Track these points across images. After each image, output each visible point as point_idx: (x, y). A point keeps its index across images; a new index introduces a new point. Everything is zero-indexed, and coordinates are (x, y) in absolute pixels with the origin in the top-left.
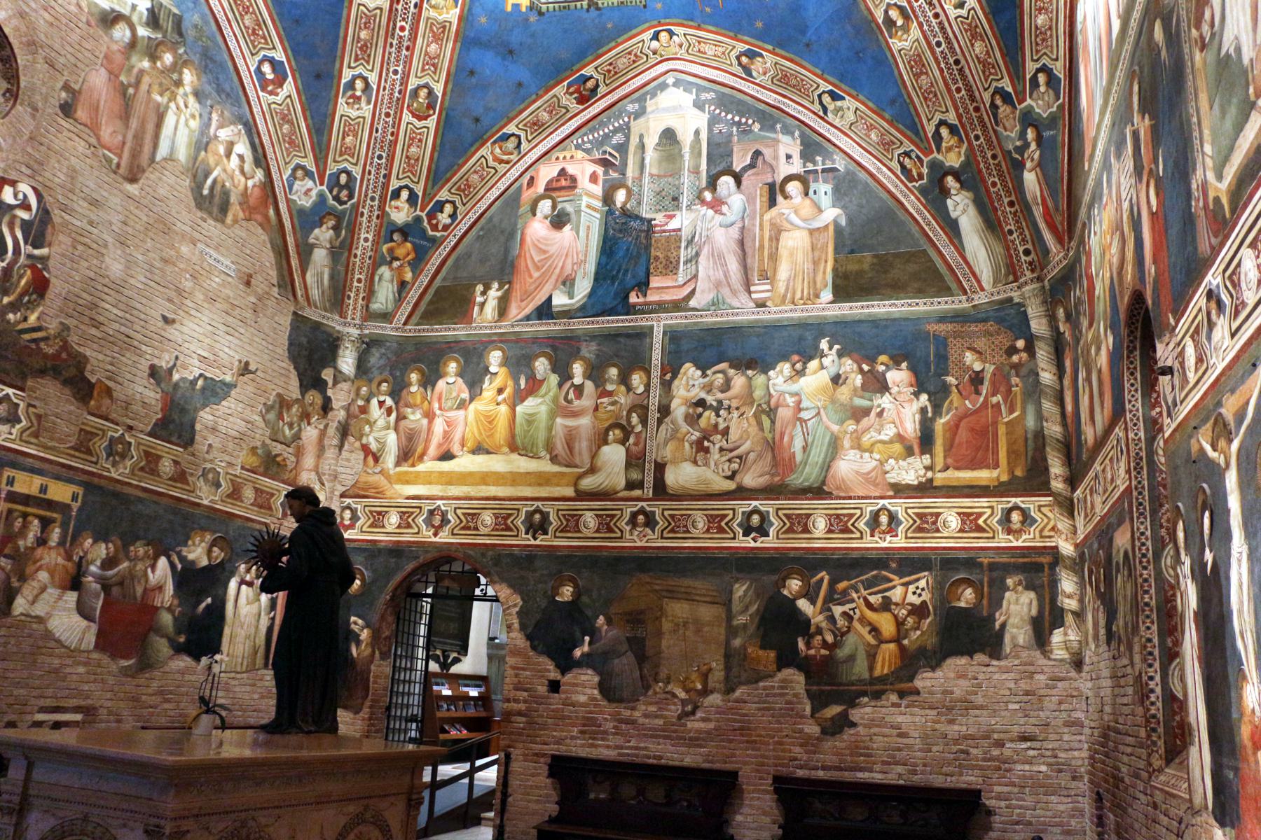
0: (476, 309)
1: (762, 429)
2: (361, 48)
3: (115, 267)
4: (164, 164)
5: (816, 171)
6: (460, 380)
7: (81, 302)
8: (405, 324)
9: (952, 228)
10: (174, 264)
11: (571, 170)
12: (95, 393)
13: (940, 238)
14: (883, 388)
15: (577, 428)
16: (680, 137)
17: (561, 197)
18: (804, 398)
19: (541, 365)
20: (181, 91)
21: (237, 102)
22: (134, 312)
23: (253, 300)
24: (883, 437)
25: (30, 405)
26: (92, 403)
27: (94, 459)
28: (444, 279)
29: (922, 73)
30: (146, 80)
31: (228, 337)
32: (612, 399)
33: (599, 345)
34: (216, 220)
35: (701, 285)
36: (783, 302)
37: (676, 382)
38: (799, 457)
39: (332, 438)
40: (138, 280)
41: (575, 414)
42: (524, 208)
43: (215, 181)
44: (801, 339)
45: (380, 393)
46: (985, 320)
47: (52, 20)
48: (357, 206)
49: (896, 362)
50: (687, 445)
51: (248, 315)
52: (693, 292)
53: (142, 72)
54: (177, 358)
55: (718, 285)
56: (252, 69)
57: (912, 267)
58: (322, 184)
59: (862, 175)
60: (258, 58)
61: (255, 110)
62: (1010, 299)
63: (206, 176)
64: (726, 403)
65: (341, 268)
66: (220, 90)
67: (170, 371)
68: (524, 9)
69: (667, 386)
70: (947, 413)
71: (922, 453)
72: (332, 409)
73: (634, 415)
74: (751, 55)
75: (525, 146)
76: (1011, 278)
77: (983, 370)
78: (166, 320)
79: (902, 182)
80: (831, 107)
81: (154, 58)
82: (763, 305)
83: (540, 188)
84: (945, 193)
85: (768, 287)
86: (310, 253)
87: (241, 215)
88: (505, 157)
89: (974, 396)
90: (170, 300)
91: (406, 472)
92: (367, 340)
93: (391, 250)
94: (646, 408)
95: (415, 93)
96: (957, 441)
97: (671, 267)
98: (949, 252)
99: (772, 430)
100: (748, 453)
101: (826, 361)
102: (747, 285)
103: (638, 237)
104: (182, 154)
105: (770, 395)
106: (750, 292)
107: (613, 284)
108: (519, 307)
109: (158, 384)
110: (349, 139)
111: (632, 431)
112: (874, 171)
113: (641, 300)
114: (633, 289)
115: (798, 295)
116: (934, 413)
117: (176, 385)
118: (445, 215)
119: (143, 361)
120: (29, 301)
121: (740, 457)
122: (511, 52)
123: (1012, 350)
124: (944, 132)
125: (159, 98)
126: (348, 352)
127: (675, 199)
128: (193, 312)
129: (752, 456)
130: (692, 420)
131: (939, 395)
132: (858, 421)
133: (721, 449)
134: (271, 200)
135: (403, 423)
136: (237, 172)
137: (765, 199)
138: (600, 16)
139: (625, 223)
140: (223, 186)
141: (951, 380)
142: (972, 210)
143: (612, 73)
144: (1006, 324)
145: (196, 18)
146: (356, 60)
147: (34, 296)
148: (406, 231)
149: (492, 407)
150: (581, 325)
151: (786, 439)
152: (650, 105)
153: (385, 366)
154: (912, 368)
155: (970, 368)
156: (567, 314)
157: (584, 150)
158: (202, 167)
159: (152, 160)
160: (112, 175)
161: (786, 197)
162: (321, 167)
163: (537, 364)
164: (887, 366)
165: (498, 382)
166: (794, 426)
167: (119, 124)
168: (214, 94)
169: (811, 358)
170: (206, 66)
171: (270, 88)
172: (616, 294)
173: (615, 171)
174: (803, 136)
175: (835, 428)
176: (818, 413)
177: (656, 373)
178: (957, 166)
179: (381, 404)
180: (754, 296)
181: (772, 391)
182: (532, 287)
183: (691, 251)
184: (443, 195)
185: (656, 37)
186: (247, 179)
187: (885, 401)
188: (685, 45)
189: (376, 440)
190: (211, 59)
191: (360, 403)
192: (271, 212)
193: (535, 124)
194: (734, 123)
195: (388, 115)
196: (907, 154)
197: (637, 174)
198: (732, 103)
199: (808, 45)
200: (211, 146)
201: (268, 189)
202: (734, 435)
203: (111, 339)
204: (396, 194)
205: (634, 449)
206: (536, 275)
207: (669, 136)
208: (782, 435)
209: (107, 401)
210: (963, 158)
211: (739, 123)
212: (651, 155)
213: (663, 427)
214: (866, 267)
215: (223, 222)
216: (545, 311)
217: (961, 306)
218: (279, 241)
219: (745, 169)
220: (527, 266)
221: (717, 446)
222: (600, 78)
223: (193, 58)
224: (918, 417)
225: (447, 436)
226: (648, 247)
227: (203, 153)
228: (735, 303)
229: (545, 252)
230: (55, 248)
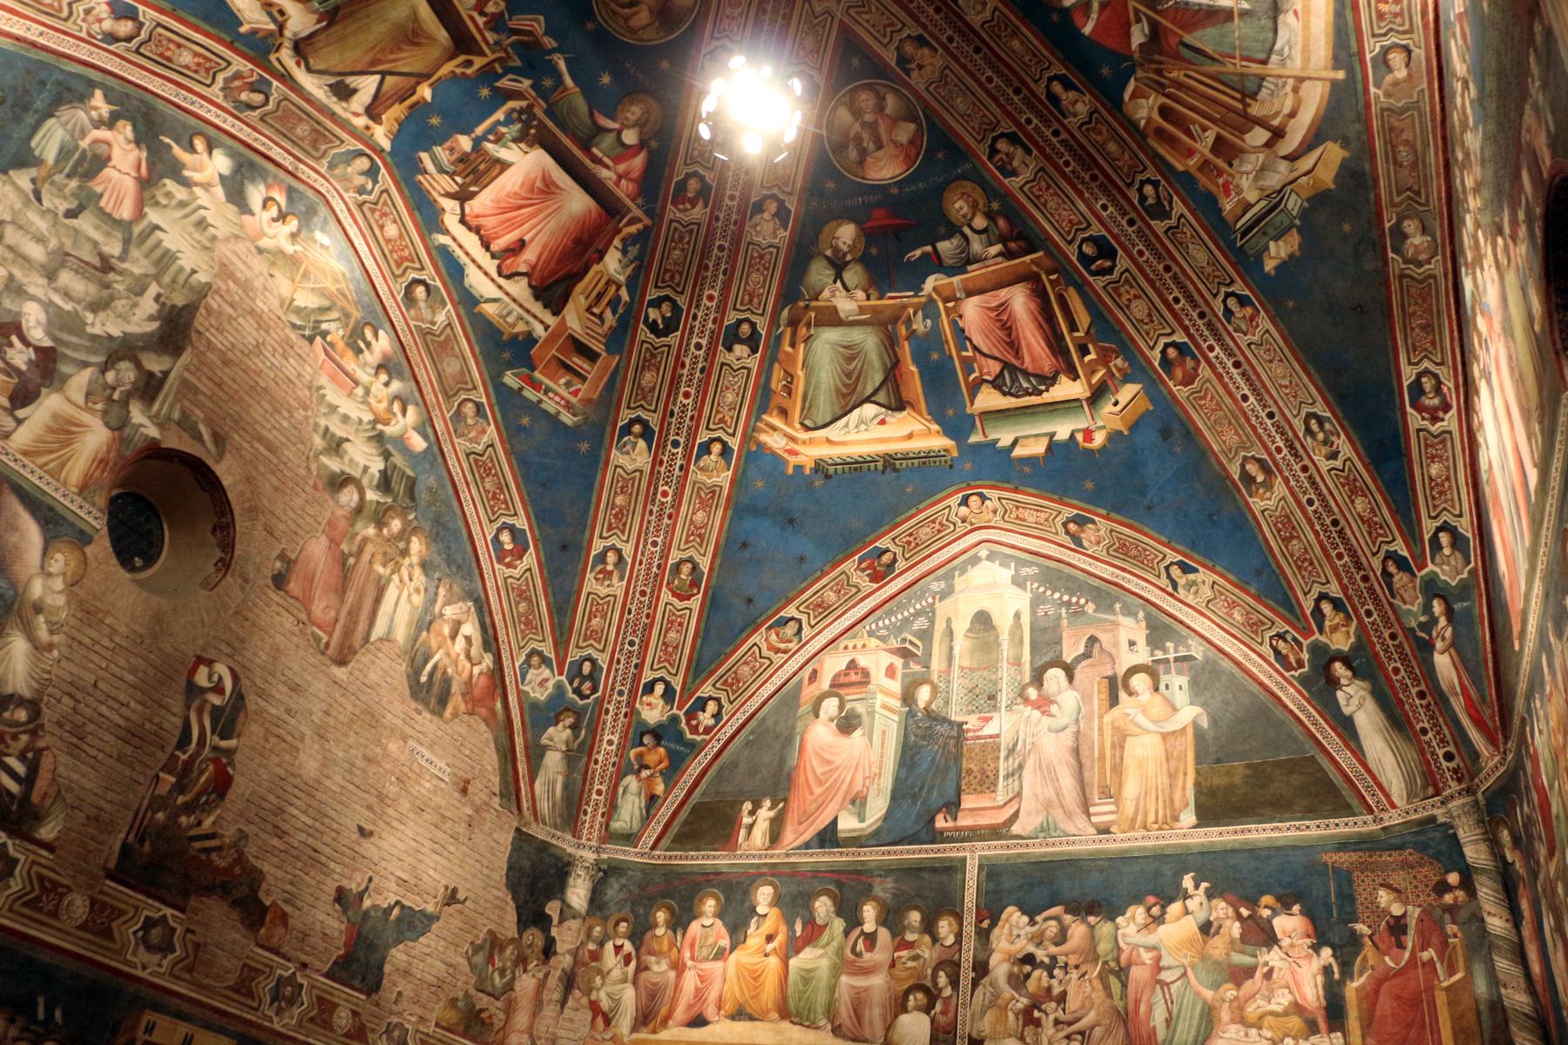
0: (743, 832)
1: (1110, 995)
2: (616, 516)
3: (310, 765)
4: (379, 644)
5: (1167, 661)
6: (719, 923)
7: (266, 805)
8: (653, 848)
9: (1346, 727)
10: (379, 764)
11: (863, 661)
12: (268, 918)
13: (1331, 740)
14: (1269, 938)
15: (866, 989)
16: (996, 621)
17: (850, 694)
18: (1164, 952)
19: (823, 907)
20: (407, 561)
22: (326, 820)
23: (469, 811)
24: (1274, 1007)
25: (188, 931)
26: (263, 931)
27: (255, 1004)
28: (703, 794)
29: (1292, 537)
30: (369, 549)
31: (438, 858)
32: (913, 953)
33: (896, 881)
34: (433, 712)
35: (1027, 805)
36: (1132, 828)
37: (996, 931)
38: (1161, 1034)
39: (553, 992)
40: (335, 781)
41: (866, 971)
42: (805, 708)
43: (435, 667)
44: (1157, 874)
45: (616, 935)
46: (1401, 847)
48: (600, 701)
49: (1285, 904)
50: (1011, 1015)
51: (461, 830)
52: (1016, 815)
53: (366, 540)
54: (370, 880)
55: (1048, 806)
56: (489, 538)
57: (1297, 780)
58: (561, 674)
59: (1226, 664)
61: (488, 585)
62: (1433, 819)
63: (426, 661)
64: (1061, 960)
65: (578, 777)
66: (450, 561)
67: (361, 896)
68: (807, 472)
69: (984, 936)
70: (1361, 974)
71: (1331, 1030)
72: (555, 953)
73: (942, 974)
74: (1081, 521)
75: (807, 632)
76: (1431, 791)
77: (1404, 915)
78: (363, 832)
79: (1277, 670)
80: (1182, 581)
81: (380, 523)
82: (1107, 831)
83: (825, 683)
84: (1333, 683)
85: (1113, 808)
86: (542, 756)
87: (463, 708)
88: (782, 646)
89: (1395, 950)
90: (369, 808)
91: (645, 1041)
92: (604, 867)
93: (640, 756)
94: (958, 965)
95: (677, 568)
96: (1378, 1013)
97: (987, 783)
98: (1345, 759)
99: (1124, 996)
100: (1092, 1028)
101: (1192, 904)
102: (1086, 805)
103: (946, 745)
104: (401, 634)
105: (1119, 949)
106: (1089, 815)
107: (914, 803)
108: (796, 831)
109: (345, 911)
110: (596, 622)
111: (939, 996)
112: (1241, 659)
113: (950, 824)
114: (939, 811)
115: (1151, 818)
116: (1342, 973)
117: (366, 914)
118: (708, 714)
119: (329, 881)
120: (206, 802)
121: (1082, 1033)
122: (791, 521)
123: (1443, 888)
124: (1326, 607)
125: (380, 569)
126: (580, 881)
127: (992, 697)
128: (395, 824)
129: (1098, 1031)
130: (1018, 982)
131: (1347, 950)
132: (1238, 985)
133: (1057, 1022)
134: (499, 691)
135: (644, 976)
136: (462, 657)
137: (1105, 695)
138: (898, 478)
139: (930, 728)
140: (445, 672)
141: (1361, 928)
142: (1370, 705)
143: (912, 545)
144: (1431, 851)
145: (432, 481)
147: (213, 796)
148: (657, 734)
149: (758, 959)
150: (873, 856)
151: (1143, 1009)
152: (959, 582)
153: (626, 900)
154: (1308, 913)
155: (1386, 912)
156: (856, 841)
157: (879, 638)
158: (422, 649)
159: (366, 640)
160: (320, 657)
161: (1131, 694)
163: (817, 904)
164: (1273, 909)
165: (767, 927)
166: (1153, 991)
167: (333, 598)
168: (444, 566)
169: (1171, 900)
172: (919, 817)
173: (917, 663)
174: (1148, 617)
175: (1209, 994)
176: (1185, 974)
177: (969, 919)
178: (1346, 649)
179: (618, 949)
180: (1094, 819)
181: (1122, 944)
182: (814, 806)
183: (1013, 763)
184: (706, 690)
185: (965, 502)
186: (473, 665)
187: (1274, 957)
188: (1000, 511)
189: (609, 995)
190: (445, 527)
191: (592, 946)
192: (499, 705)
193: (820, 606)
194: (1063, 603)
195: (643, 593)
196: (1281, 636)
197: (944, 666)
198: (1059, 579)
199: (1149, 508)
200: (435, 626)
201: (497, 677)
202: (1073, 1003)
203: (296, 853)
204: (649, 688)
205: (942, 1019)
206: (818, 791)
207: (983, 620)
208: (1137, 1002)
209: (280, 931)
210: (1352, 639)
211: (1069, 604)
212: (961, 644)
213: (979, 991)
214: (1237, 780)
215: (441, 715)
216: (828, 837)
217: (1366, 829)
218: (505, 741)
219: (1078, 659)
220: (807, 781)
221: (1052, 1017)
222: (898, 551)
224: (1320, 979)
225: (699, 994)
226: (958, 757)
227: (425, 633)
228: (1071, 829)
229: (829, 762)
230: (243, 740)
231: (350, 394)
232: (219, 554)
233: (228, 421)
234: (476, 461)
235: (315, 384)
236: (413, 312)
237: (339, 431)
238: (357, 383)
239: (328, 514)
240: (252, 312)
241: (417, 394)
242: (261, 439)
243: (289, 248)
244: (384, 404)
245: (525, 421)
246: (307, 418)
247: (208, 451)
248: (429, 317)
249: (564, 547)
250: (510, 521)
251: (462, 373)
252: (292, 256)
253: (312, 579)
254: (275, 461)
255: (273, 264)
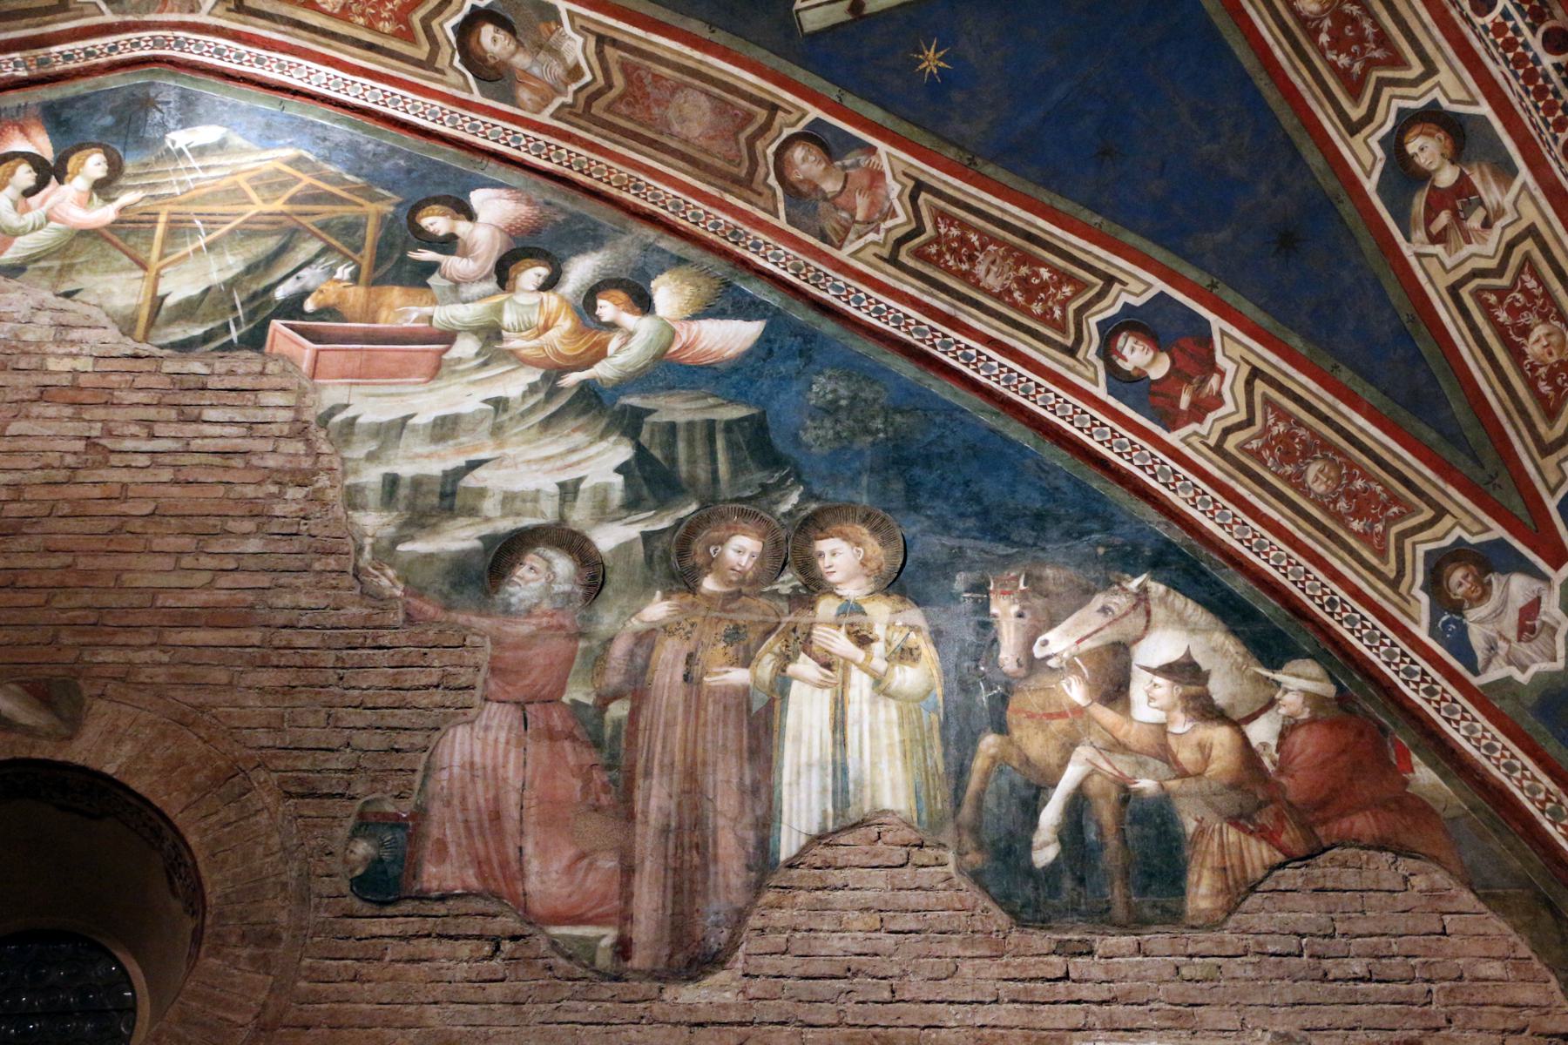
2: (1338, 43)
20: (826, 607)
21: (1095, 513)
30: (668, 660)
34: (1135, 923)
43: (1078, 803)
47: (287, 677)
53: (647, 639)
60: (1090, 351)
61: (1178, 500)
66: (995, 524)
87: (1259, 853)
125: (738, 676)
136: (1181, 724)
140: (1126, 795)
145: (823, 387)
146: (1355, 93)
159: (763, 861)
160: (608, 989)
162: (1517, 507)
167: (594, 829)
168: (972, 547)
170: (912, 489)
171: (1185, 401)
186: (1237, 725)
192: (1424, 776)
215: (1173, 916)
223: (845, 495)
231: (436, 371)
232: (190, 924)
233: (66, 638)
234: (919, 254)
235: (309, 416)
236: (524, 95)
237: (431, 462)
238: (447, 337)
239: (483, 657)
240: (44, 394)
241: (669, 244)
242: (187, 619)
243: (103, 214)
244: (565, 324)
245: (932, 61)
246: (314, 498)
247: (29, 731)
248: (559, 71)
249: (1287, 241)
250: (1110, 308)
251: (721, 107)
252: (117, 226)
253: (496, 816)
254: (256, 636)
255: (66, 270)
